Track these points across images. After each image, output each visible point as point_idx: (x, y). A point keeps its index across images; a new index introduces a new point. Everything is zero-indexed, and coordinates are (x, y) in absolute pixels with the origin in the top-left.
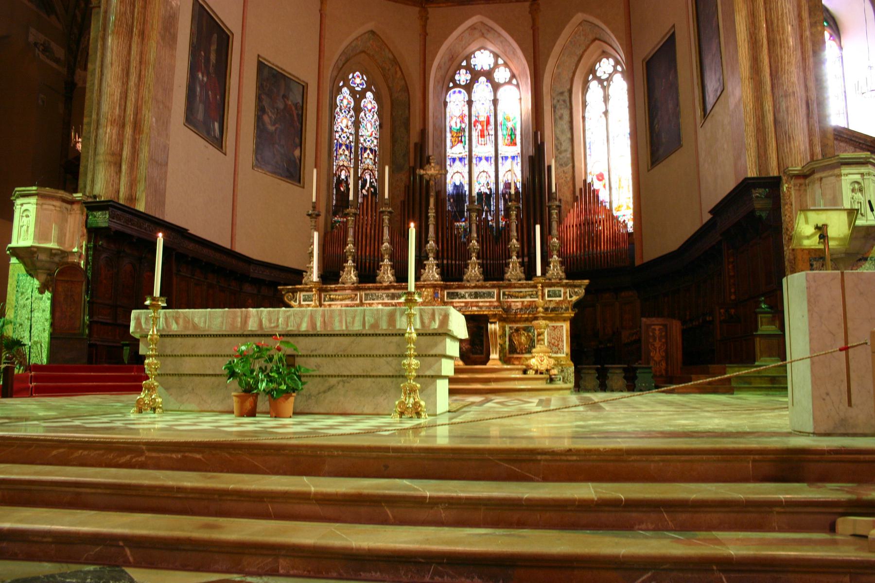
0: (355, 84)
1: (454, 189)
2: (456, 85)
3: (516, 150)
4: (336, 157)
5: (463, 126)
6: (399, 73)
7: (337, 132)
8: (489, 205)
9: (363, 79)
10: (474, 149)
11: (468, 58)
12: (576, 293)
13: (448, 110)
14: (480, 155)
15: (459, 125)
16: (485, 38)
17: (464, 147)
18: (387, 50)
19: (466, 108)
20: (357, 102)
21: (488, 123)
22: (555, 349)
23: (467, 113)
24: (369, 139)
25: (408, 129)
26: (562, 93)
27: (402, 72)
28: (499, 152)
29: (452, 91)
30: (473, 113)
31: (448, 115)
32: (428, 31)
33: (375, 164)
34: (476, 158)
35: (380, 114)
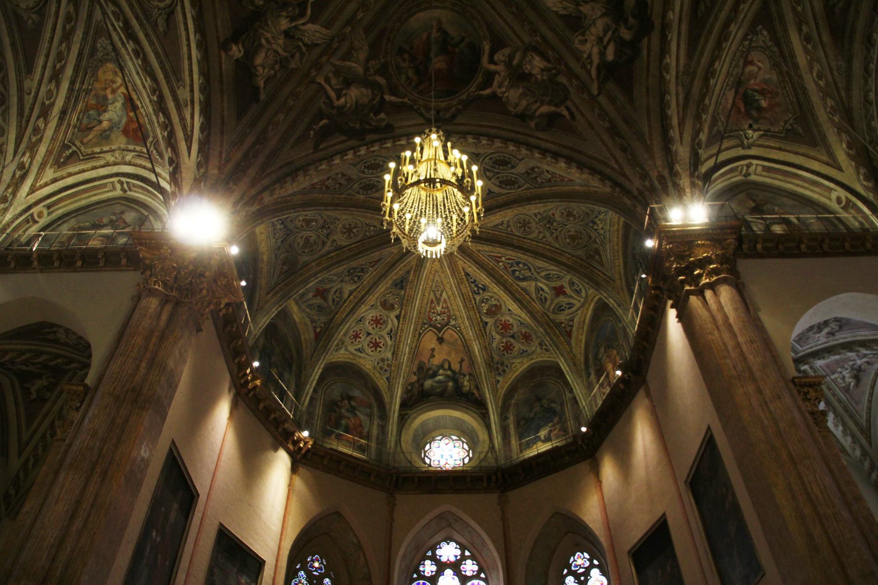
0: (313, 567)
6: (362, 559)
9: (322, 563)
11: (434, 548)
16: (452, 528)
27: (365, 557)
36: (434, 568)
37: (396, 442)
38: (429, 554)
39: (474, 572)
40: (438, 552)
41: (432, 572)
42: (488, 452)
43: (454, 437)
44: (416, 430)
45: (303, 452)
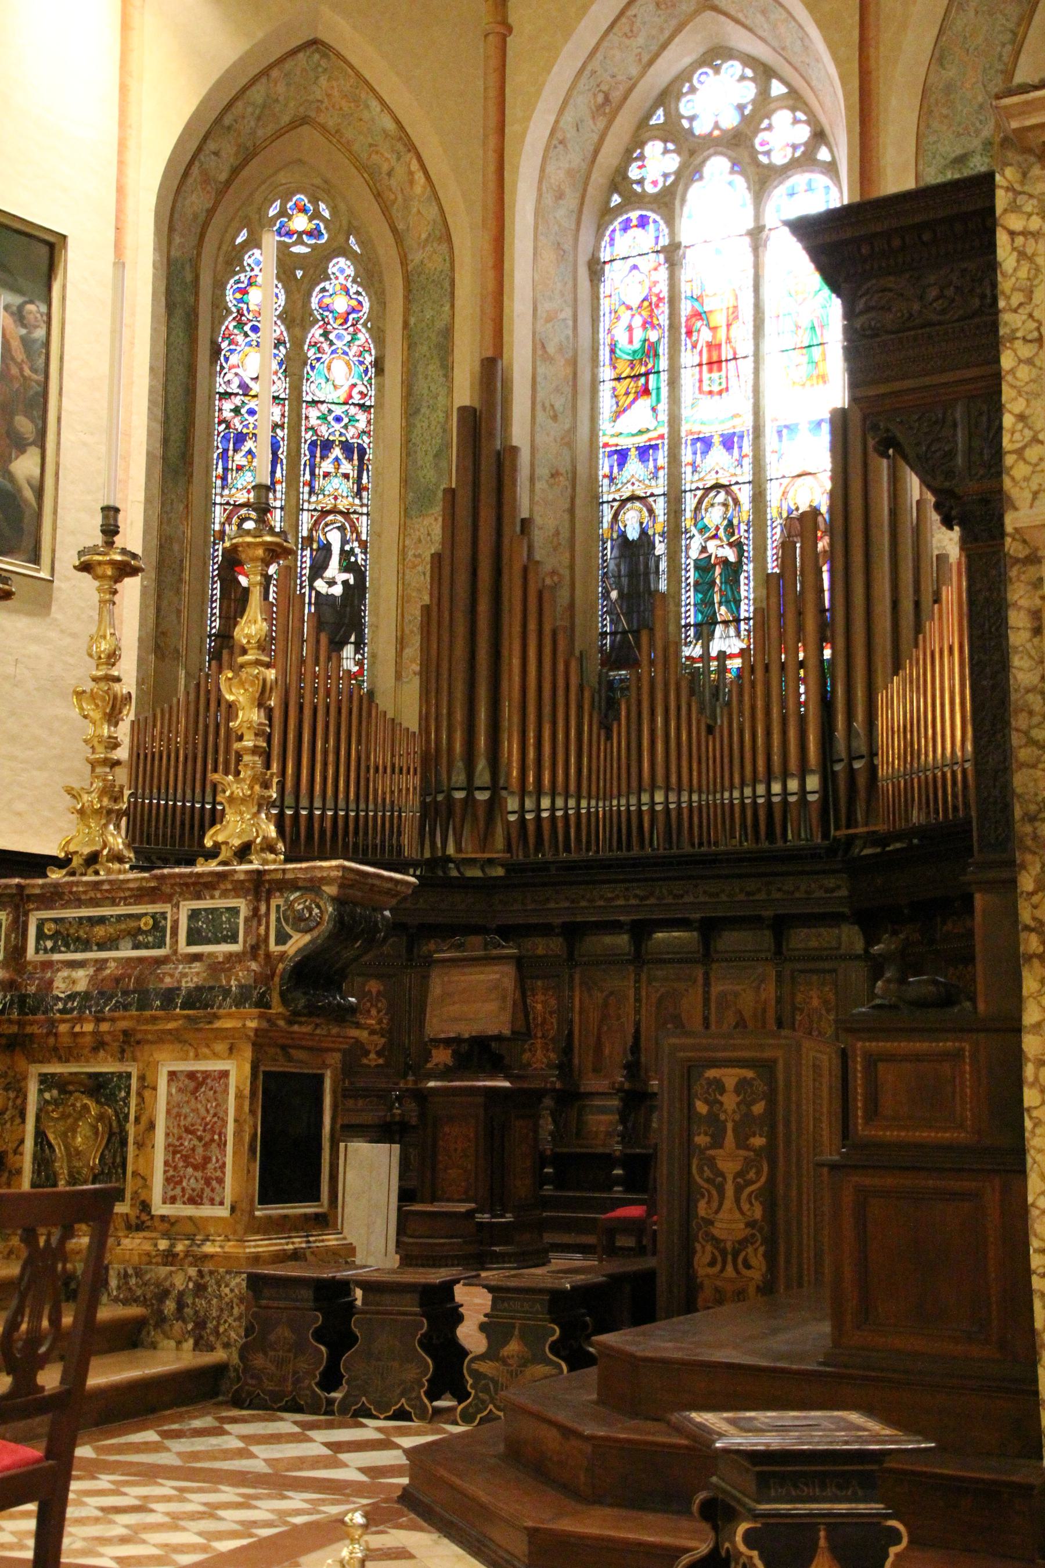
1: (622, 556)
2: (633, 199)
4: (224, 479)
5: (653, 336)
6: (419, 177)
7: (226, 395)
10: (685, 412)
12: (300, 922)
13: (605, 289)
14: (706, 431)
15: (638, 335)
17: (654, 409)
18: (374, 104)
19: (662, 275)
21: (734, 314)
22: (192, 1181)
23: (665, 294)
24: (338, 410)
25: (447, 368)
29: (616, 224)
30: (685, 289)
32: (511, 20)
33: (358, 494)
36: (673, 162)
38: (658, 118)
39: (795, 147)
40: (685, 107)
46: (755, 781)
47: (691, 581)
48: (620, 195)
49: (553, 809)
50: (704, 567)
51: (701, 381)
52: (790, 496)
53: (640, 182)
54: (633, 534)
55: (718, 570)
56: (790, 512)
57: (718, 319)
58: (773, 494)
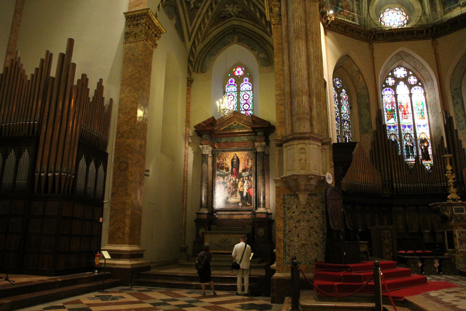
0: (336, 84)
3: (426, 121)
5: (393, 108)
6: (362, 78)
8: (413, 153)
9: (340, 82)
11: (392, 72)
13: (384, 99)
14: (405, 124)
15: (391, 108)
17: (395, 120)
18: (355, 66)
19: (394, 99)
20: (339, 94)
21: (407, 107)
23: (395, 101)
24: (346, 115)
25: (369, 110)
26: (456, 89)
28: (416, 123)
29: (385, 89)
30: (398, 101)
31: (384, 102)
32: (374, 56)
34: (403, 126)
35: (350, 101)
36: (394, 81)
37: (367, 14)
38: (390, 74)
39: (415, 82)
41: (393, 83)
42: (421, 16)
43: (397, 9)
44: (376, 6)
45: (329, 23)
46: (444, 182)
47: (405, 148)
48: (385, 85)
49: (402, 185)
50: (407, 146)
51: (403, 116)
52: (421, 136)
53: (388, 83)
54: (393, 140)
55: (409, 147)
56: (421, 139)
57: (405, 107)
58: (418, 135)
